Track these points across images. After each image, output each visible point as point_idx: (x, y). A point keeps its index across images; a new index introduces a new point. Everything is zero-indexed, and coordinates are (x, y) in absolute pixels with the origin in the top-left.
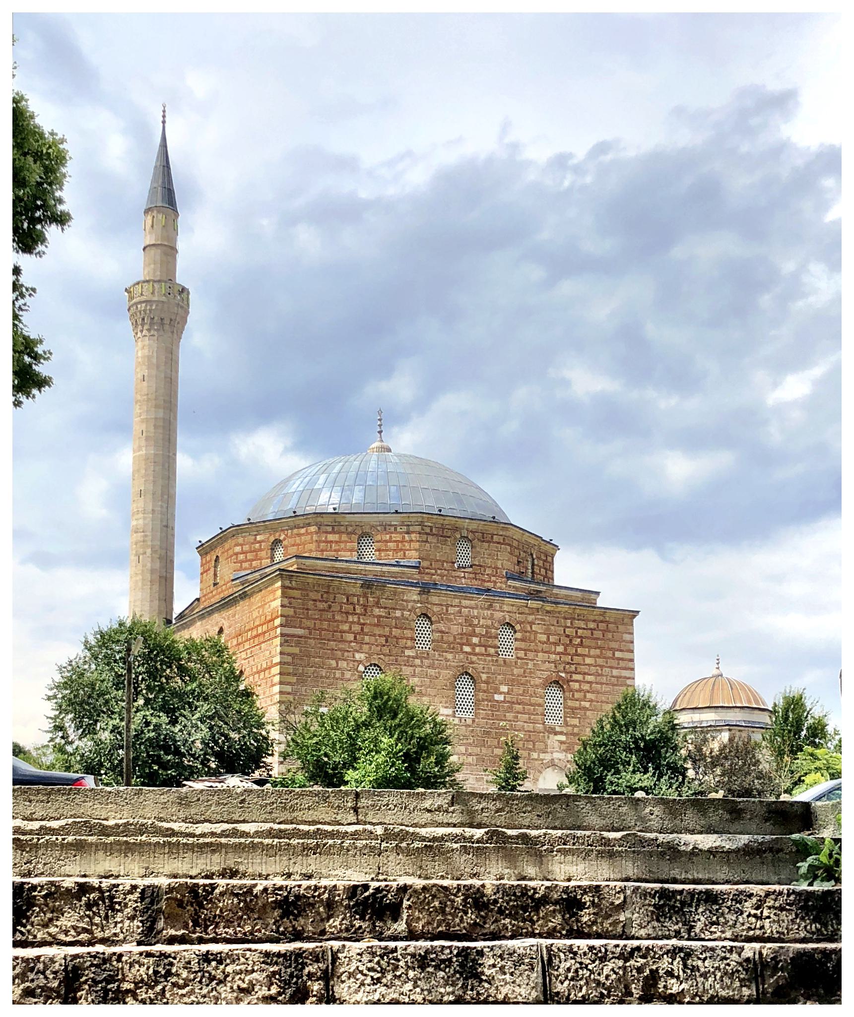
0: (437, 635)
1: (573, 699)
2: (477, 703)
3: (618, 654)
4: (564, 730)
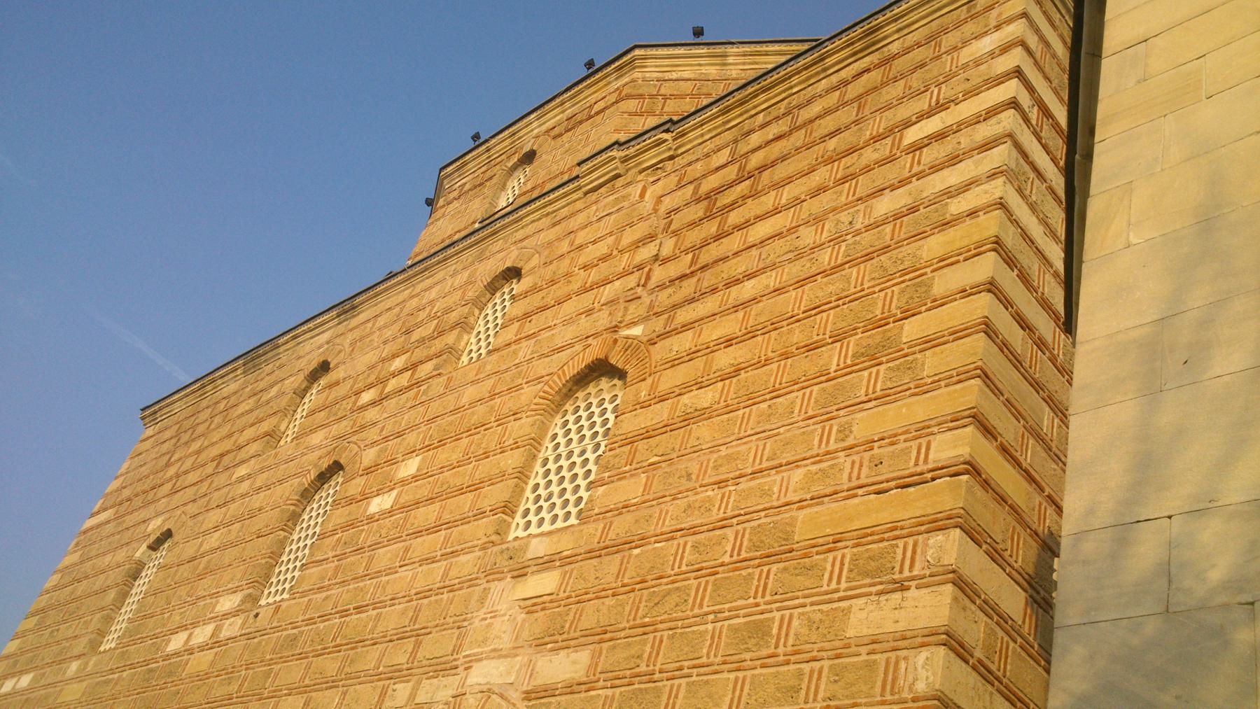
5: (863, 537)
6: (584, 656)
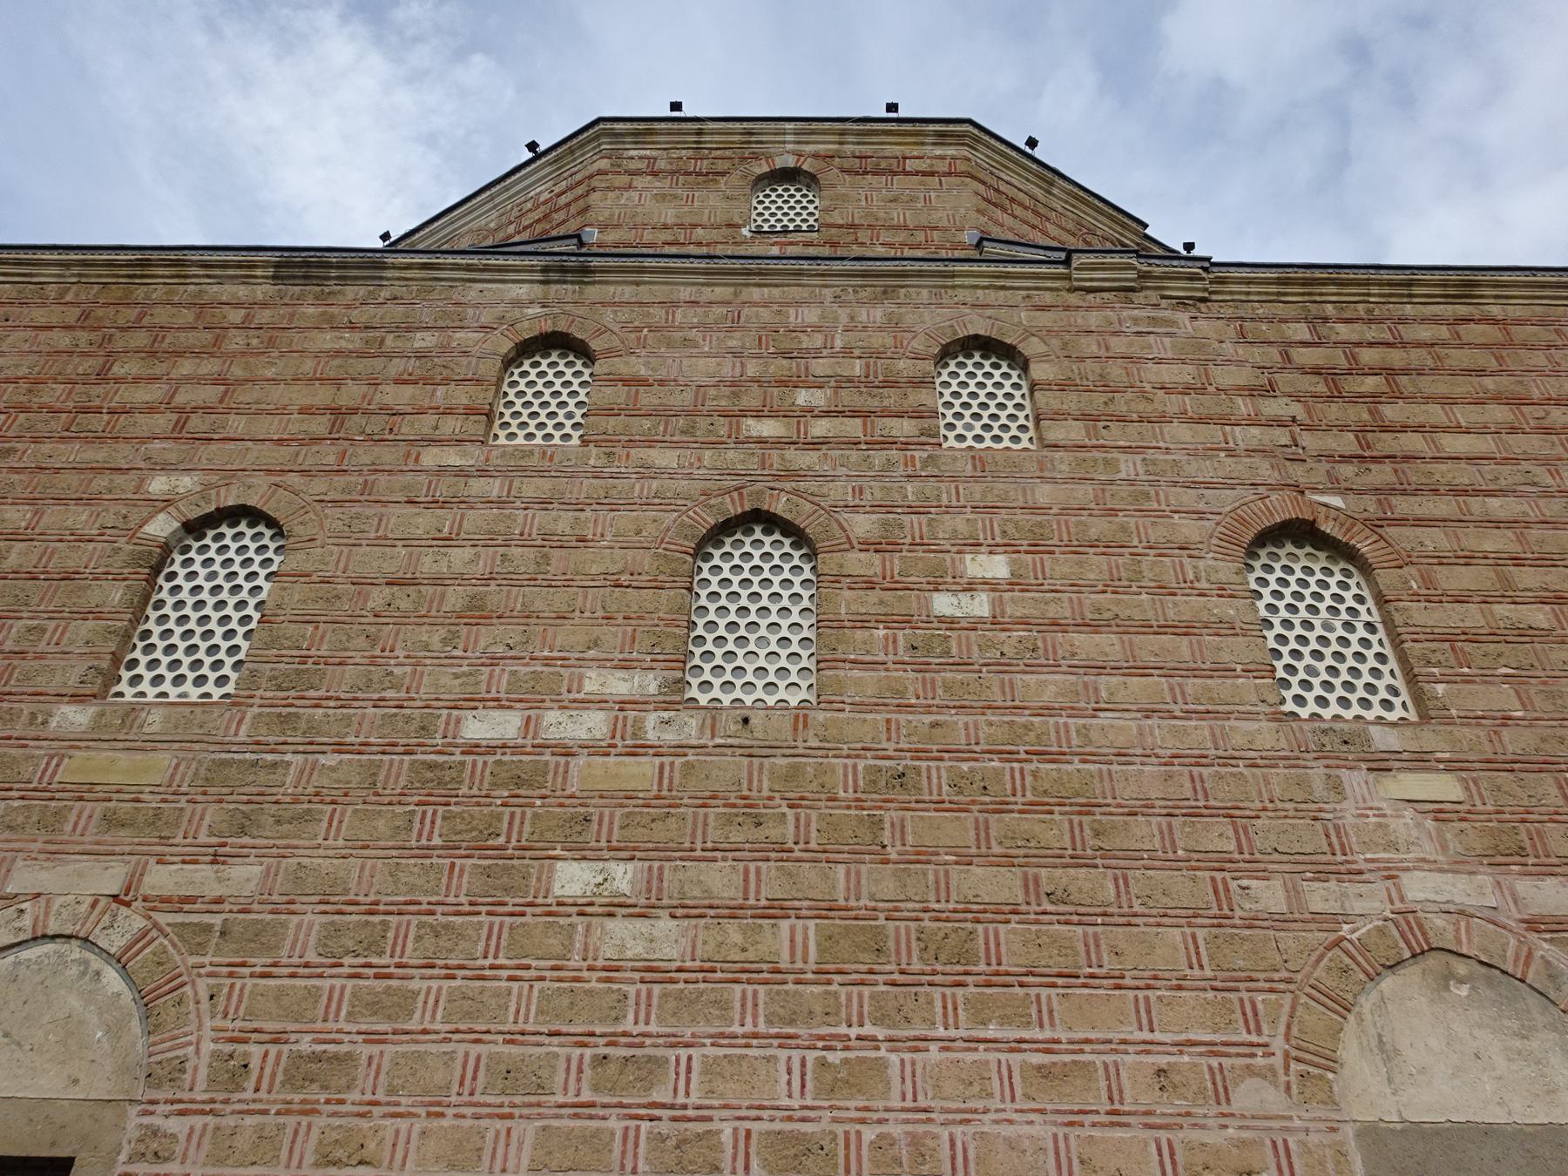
1: (1433, 597)
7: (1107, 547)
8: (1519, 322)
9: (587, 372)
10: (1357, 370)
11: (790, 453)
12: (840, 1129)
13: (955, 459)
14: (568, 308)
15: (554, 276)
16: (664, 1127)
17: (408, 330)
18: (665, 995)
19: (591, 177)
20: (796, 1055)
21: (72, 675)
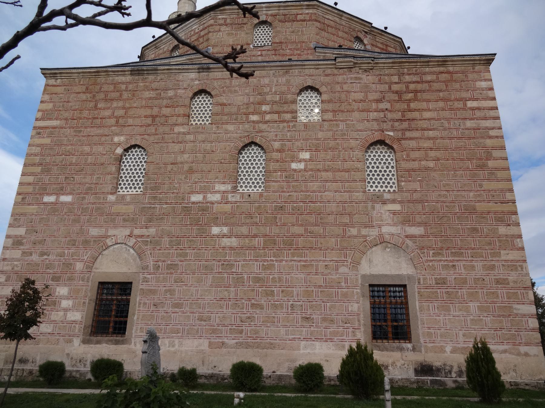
0: (218, 109)
2: (268, 173)
3: (470, 104)
4: (398, 197)
5: (495, 213)
6: (422, 229)
7: (333, 149)
8: (457, 73)
9: (211, 100)
10: (408, 91)
11: (260, 125)
12: (266, 276)
13: (300, 125)
14: (205, 81)
15: (201, 70)
16: (235, 276)
17: (166, 90)
18: (234, 253)
19: (209, 26)
20: (258, 263)
21: (109, 188)
